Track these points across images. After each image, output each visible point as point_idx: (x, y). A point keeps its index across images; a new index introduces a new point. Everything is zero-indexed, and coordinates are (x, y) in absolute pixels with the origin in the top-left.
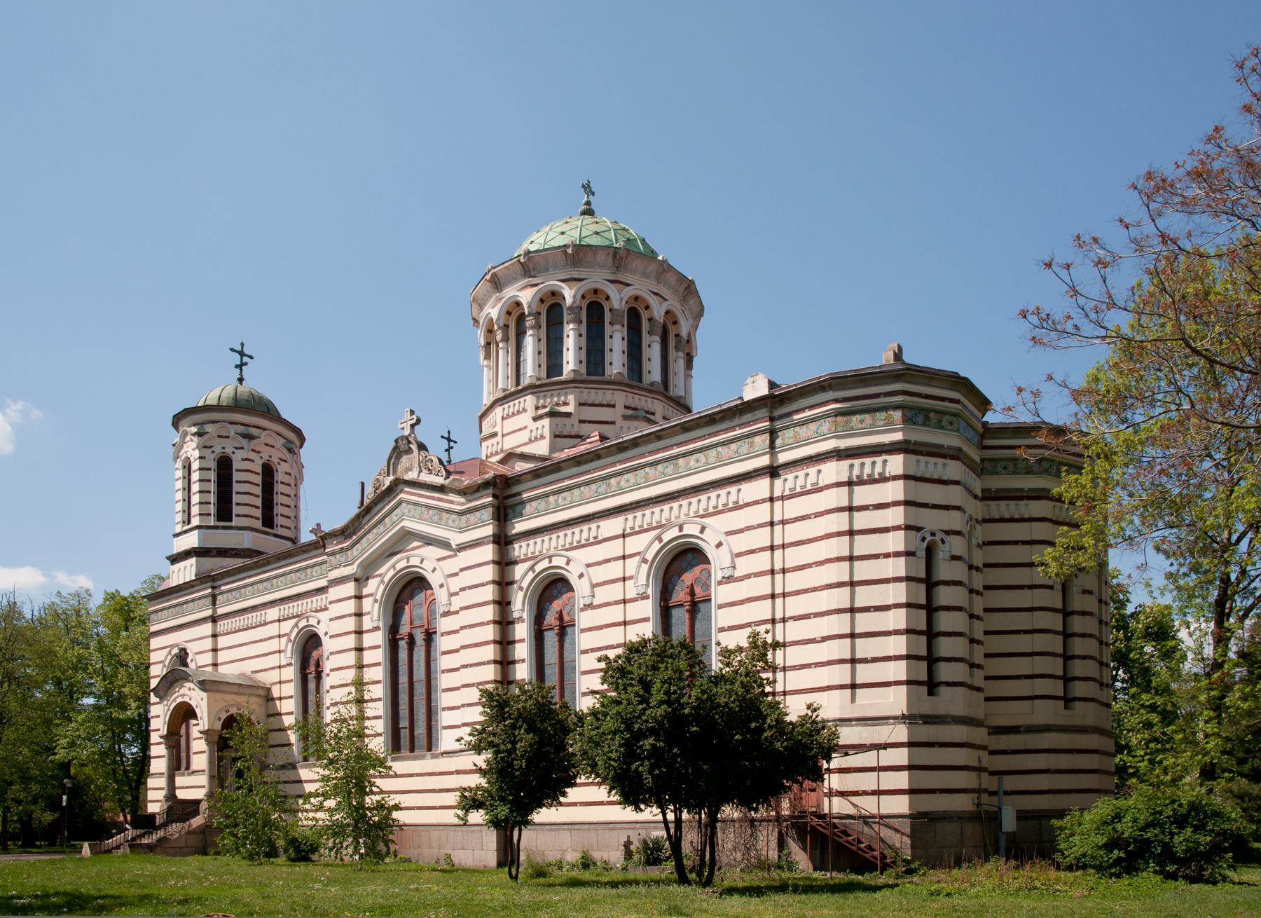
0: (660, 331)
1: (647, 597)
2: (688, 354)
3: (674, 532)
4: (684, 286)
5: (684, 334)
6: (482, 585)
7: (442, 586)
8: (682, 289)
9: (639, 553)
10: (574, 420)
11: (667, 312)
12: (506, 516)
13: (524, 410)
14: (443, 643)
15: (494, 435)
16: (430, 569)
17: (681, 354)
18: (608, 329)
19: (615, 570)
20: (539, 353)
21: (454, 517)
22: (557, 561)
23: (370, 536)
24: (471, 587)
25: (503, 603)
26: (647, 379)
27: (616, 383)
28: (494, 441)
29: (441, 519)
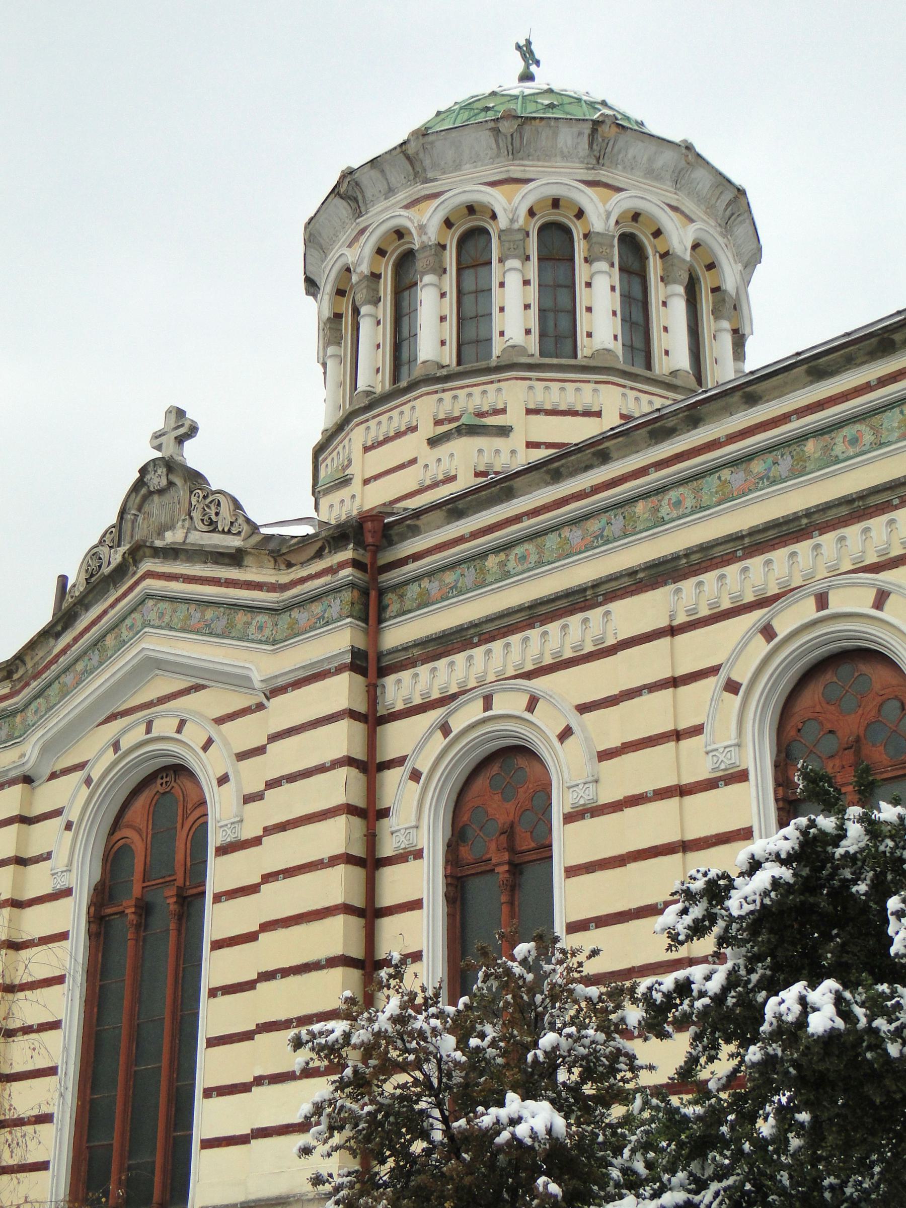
0: (685, 277)
1: (742, 776)
2: (735, 331)
3: (807, 610)
4: (728, 196)
5: (730, 284)
6: (322, 769)
7: (223, 780)
8: (721, 204)
9: (714, 670)
10: (517, 440)
11: (696, 246)
12: (382, 608)
13: (413, 429)
14: (218, 920)
15: (345, 482)
16: (197, 745)
17: (726, 324)
18: (582, 272)
19: (652, 714)
20: (443, 319)
21: (261, 618)
22: (509, 703)
23: (68, 679)
24: (292, 778)
25: (370, 813)
26: (662, 366)
27: (598, 369)
28: (344, 493)
29: (231, 625)
